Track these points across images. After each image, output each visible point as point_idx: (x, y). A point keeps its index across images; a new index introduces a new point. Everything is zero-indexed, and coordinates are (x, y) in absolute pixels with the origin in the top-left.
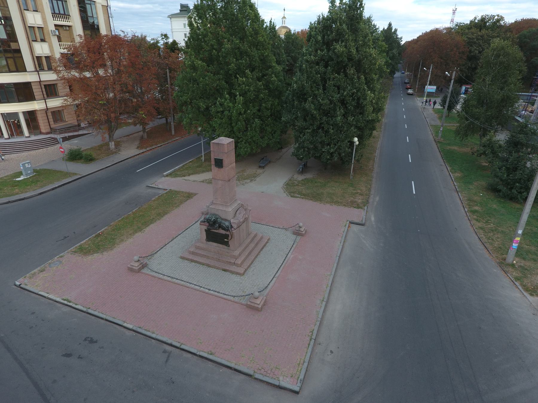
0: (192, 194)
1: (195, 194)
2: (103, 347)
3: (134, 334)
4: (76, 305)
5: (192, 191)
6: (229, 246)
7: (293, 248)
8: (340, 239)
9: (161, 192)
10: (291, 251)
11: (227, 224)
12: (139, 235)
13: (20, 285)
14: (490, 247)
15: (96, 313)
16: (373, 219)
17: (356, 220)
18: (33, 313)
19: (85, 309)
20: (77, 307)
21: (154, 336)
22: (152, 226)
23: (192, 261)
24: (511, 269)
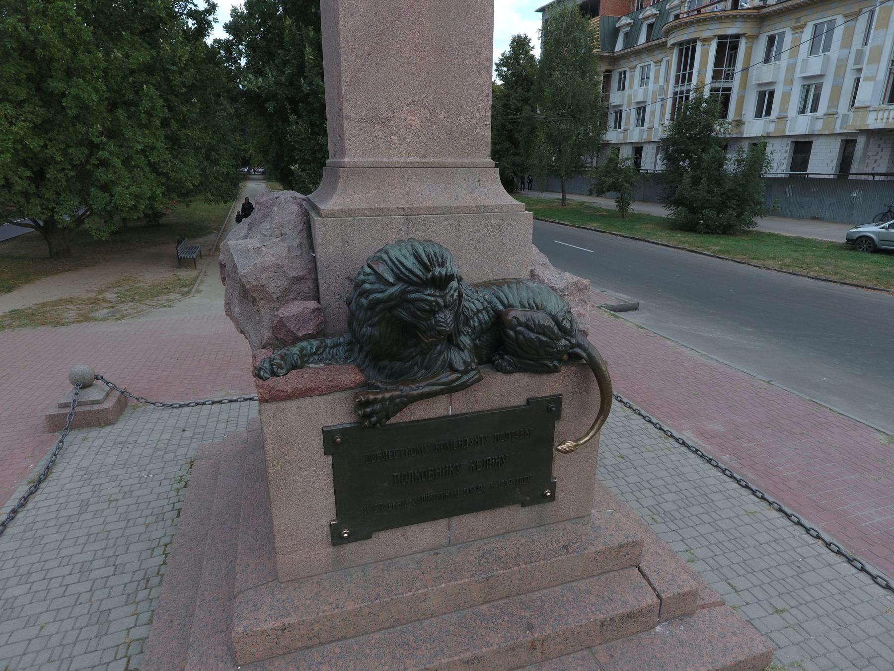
6: (552, 498)
7: (643, 412)
8: (668, 341)
10: (654, 420)
11: (553, 305)
14: (870, 284)
16: (625, 296)
17: (614, 303)
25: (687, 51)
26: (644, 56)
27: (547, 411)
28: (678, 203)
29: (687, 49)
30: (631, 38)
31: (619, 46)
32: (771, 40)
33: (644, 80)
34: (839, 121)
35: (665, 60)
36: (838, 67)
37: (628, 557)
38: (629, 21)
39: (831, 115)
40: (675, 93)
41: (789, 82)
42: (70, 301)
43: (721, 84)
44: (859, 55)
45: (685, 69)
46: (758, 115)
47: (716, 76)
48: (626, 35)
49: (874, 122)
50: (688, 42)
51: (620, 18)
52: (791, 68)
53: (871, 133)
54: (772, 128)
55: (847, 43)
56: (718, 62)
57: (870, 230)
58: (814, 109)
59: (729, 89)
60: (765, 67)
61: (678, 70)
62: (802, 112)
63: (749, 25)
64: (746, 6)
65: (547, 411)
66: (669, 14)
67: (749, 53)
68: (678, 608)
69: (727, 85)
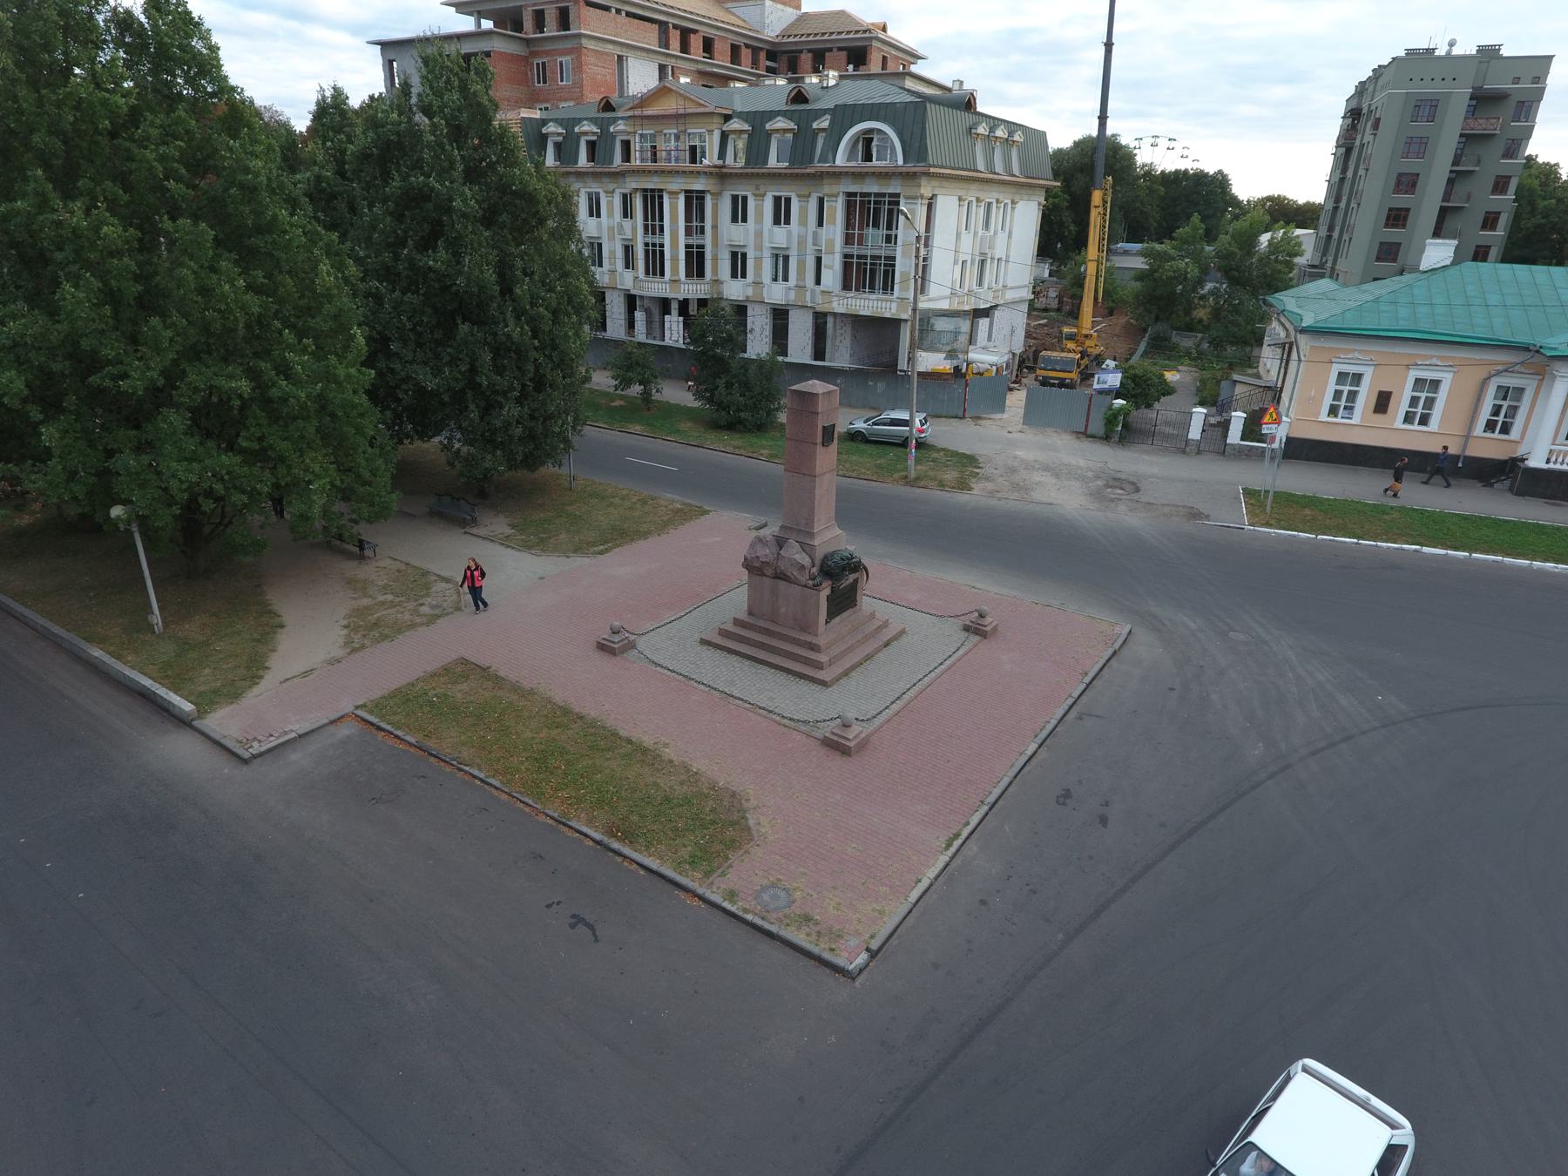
0: (446, 670)
1: (464, 661)
2: (1080, 782)
3: (1044, 748)
4: (968, 823)
5: (430, 668)
9: (346, 730)
12: (668, 753)
13: (868, 950)
15: (997, 792)
18: (983, 902)
19: (986, 808)
20: (974, 820)
21: (1054, 722)
22: (623, 733)
23: (846, 673)
24: (923, 483)
25: (653, 200)
26: (589, 181)
27: (856, 581)
28: (710, 401)
29: (653, 198)
30: (565, 151)
31: (550, 160)
32: (735, 198)
33: (595, 211)
34: (808, 294)
35: (618, 191)
36: (799, 243)
37: (873, 616)
38: (560, 130)
39: (800, 287)
40: (647, 245)
41: (759, 247)
42: (366, 608)
43: (694, 241)
44: (815, 233)
45: (653, 219)
46: (734, 275)
47: (688, 232)
48: (558, 146)
49: (839, 306)
50: (653, 190)
51: (544, 122)
52: (759, 234)
53: (835, 315)
54: (750, 292)
55: (803, 222)
56: (688, 219)
57: (860, 425)
58: (786, 279)
59: (703, 247)
60: (733, 227)
61: (646, 219)
62: (775, 279)
63: (712, 181)
64: (706, 162)
65: (856, 581)
66: (613, 137)
67: (718, 209)
68: (886, 624)
69: (700, 242)
